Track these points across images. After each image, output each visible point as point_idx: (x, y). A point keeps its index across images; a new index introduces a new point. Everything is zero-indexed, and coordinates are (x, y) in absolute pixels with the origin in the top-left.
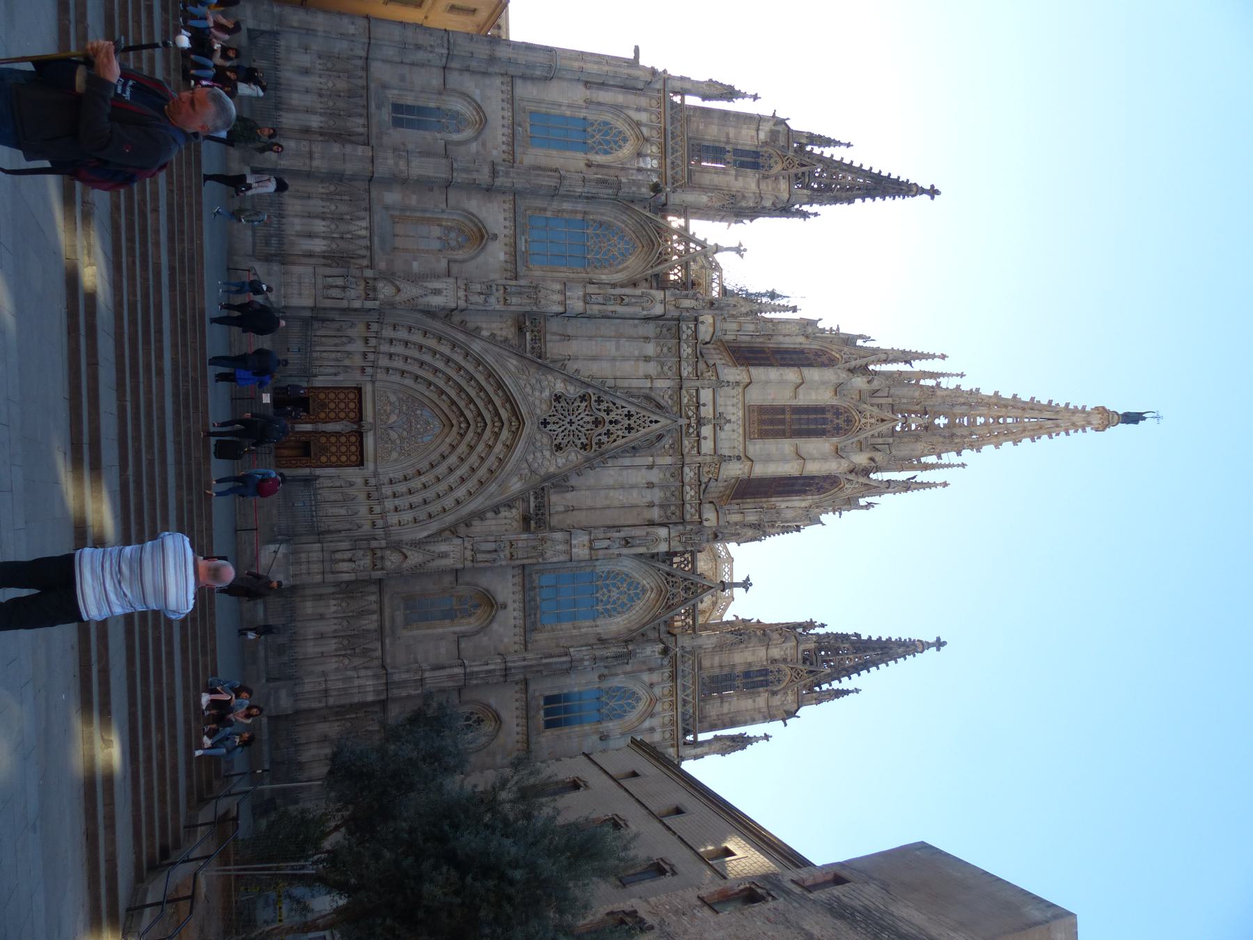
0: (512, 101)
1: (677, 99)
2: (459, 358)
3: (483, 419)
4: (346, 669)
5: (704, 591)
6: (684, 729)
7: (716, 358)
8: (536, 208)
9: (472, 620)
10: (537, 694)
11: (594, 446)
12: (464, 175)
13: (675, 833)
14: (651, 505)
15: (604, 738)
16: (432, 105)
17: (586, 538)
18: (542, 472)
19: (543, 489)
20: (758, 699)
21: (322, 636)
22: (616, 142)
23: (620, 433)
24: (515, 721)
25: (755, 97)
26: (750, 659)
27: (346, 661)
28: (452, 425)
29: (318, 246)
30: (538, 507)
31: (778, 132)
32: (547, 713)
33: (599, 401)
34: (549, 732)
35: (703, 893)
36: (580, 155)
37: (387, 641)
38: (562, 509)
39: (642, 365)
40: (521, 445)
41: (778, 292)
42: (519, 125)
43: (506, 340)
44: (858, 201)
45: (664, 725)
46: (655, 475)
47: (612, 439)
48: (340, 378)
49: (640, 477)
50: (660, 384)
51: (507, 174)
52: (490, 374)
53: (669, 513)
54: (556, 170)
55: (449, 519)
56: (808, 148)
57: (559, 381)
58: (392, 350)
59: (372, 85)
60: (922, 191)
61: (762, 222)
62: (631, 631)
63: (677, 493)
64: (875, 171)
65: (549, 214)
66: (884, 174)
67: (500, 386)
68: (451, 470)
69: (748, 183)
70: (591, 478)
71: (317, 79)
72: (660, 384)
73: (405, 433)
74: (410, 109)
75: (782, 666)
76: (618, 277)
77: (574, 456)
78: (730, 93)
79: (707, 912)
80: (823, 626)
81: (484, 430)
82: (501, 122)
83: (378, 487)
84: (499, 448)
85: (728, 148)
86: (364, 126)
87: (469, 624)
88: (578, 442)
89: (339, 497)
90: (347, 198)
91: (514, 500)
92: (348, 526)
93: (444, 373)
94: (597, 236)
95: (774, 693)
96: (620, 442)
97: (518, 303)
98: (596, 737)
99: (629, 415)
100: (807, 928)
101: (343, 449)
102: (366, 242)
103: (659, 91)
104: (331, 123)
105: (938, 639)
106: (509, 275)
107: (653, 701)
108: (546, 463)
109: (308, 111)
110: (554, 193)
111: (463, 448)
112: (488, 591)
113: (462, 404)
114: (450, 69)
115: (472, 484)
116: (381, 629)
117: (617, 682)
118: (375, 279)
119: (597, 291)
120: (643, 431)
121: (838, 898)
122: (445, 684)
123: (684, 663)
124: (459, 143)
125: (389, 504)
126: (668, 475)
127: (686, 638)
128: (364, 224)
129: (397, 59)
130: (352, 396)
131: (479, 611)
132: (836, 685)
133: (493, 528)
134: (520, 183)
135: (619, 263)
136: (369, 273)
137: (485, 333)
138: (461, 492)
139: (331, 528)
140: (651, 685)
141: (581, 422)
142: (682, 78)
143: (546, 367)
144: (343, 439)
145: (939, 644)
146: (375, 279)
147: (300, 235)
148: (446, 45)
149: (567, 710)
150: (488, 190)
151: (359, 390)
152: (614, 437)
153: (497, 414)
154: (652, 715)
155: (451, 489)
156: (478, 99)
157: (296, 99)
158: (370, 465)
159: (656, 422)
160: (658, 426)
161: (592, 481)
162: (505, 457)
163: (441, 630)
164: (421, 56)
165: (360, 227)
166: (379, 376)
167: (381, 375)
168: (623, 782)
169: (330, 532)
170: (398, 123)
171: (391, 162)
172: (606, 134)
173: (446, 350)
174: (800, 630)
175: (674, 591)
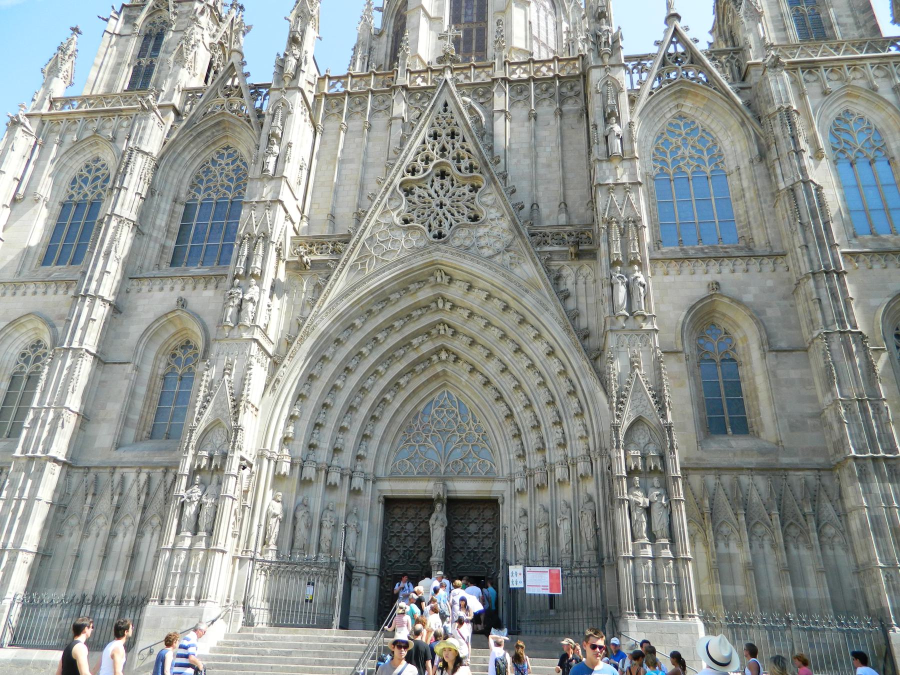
3: (433, 325)
9: (737, 335)
14: (561, 113)
17: (604, 165)
19: (533, 235)
22: (98, 170)
23: (457, 145)
27: (830, 530)
30: (562, 242)
33: (413, 171)
37: (785, 460)
39: (374, 133)
45: (889, 76)
46: (521, 112)
47: (466, 154)
48: (365, 525)
53: (572, 93)
55: (578, 362)
58: (325, 445)
62: (743, 124)
68: (505, 369)
73: (454, 439)
82: (39, 296)
83: (529, 474)
84: (475, 300)
87: (745, 339)
88: (469, 195)
89: (542, 534)
91: (548, 271)
92: (587, 519)
93: (365, 378)
99: (435, 136)
101: (473, 528)
107: (850, 92)
108: (495, 232)
111: (476, 355)
113: (413, 356)
119: (259, 165)
120: (457, 119)
125: (555, 455)
126: (520, 97)
128: (131, 476)
130: (398, 512)
131: (723, 325)
133: (591, 300)
135: (245, 164)
138: (537, 350)
139: (591, 546)
141: (441, 193)
144: (459, 528)
147: (129, 575)
151: (390, 503)
152: (463, 153)
155: (532, 366)
158: (496, 488)
159: (446, 105)
165: (134, 481)
166: (369, 469)
167: (368, 466)
169: (598, 548)
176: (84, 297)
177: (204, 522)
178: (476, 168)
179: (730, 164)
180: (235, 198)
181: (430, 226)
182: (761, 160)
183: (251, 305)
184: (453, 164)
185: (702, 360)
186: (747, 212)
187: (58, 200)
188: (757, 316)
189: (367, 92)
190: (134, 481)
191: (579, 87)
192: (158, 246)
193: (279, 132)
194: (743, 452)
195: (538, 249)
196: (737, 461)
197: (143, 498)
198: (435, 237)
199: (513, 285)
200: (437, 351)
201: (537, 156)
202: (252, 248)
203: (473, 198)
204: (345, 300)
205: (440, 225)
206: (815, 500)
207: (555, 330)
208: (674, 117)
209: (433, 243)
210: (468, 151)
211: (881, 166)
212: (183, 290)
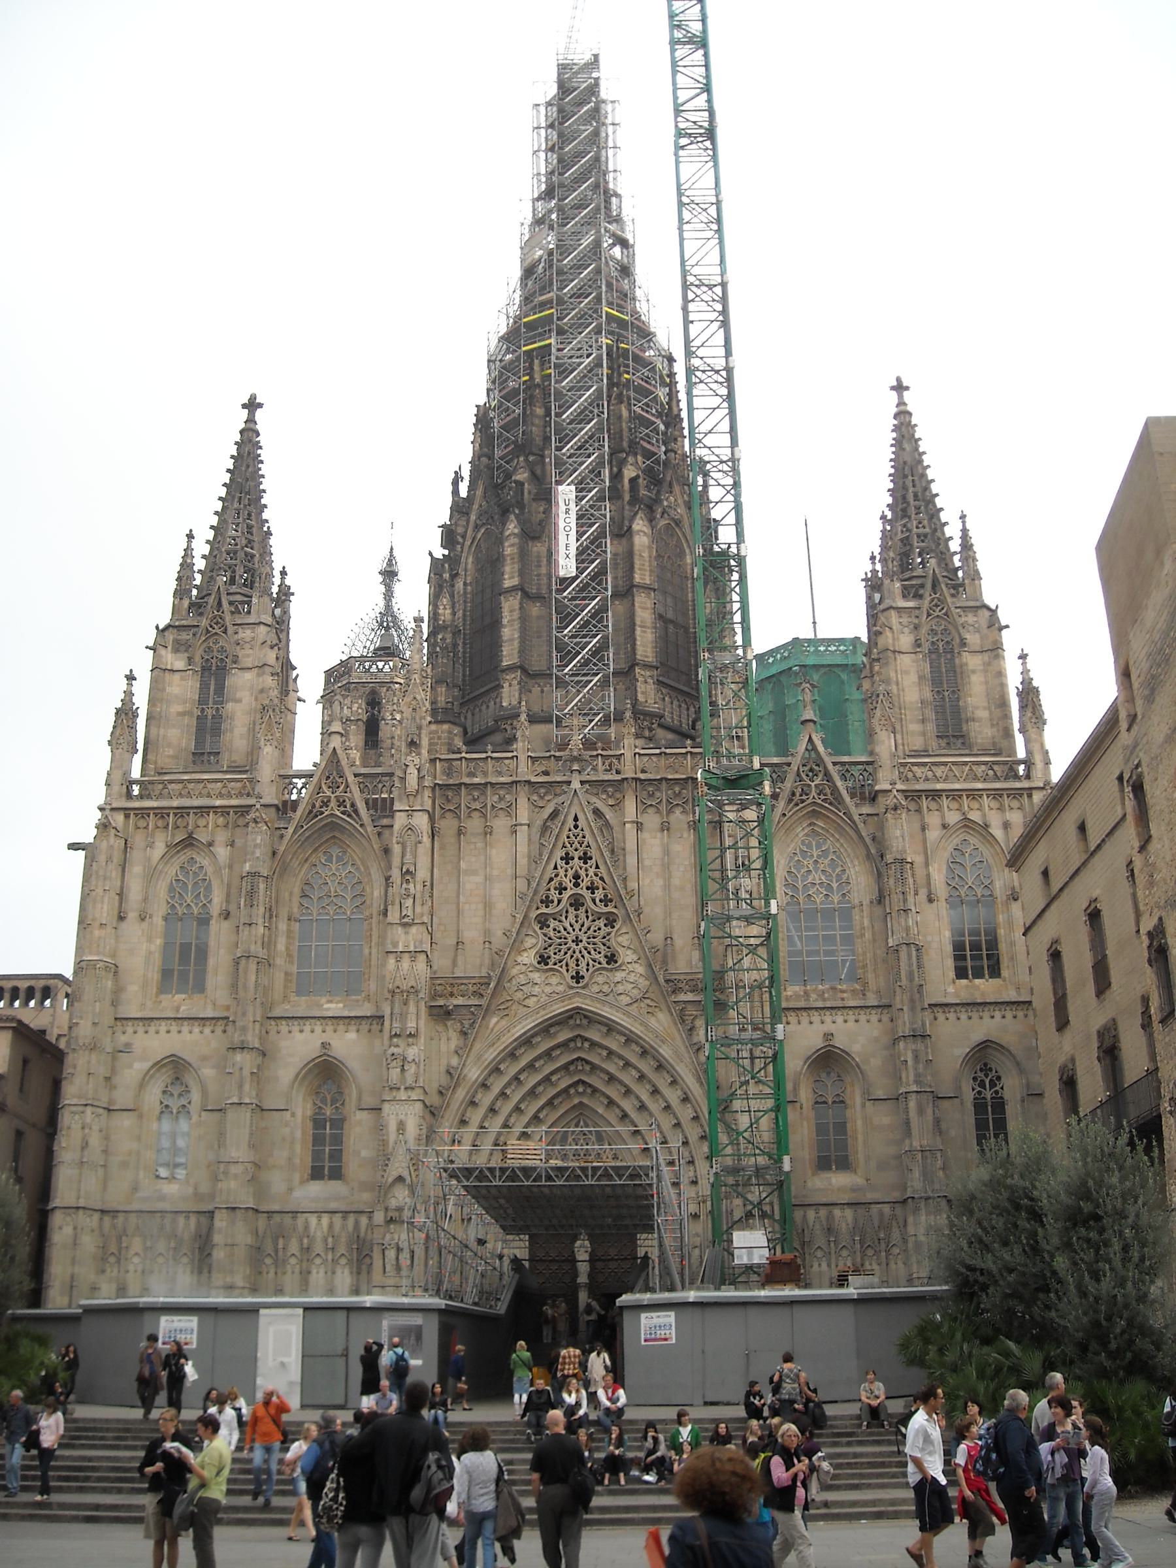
1: (136, 790)
2: (485, 1100)
3: (572, 1062)
5: (814, 748)
6: (1006, 778)
7: (486, 714)
8: (285, 987)
9: (848, 1079)
10: (951, 989)
11: (610, 909)
12: (247, 1087)
13: (1103, 840)
18: (643, 983)
19: (667, 981)
20: (971, 667)
23: (591, 873)
24: (987, 1019)
25: (131, 678)
26: (913, 677)
28: (581, 1102)
31: (177, 642)
32: (978, 974)
33: (547, 902)
34: (1005, 973)
35: (1137, 845)
37: (870, 1196)
38: (696, 955)
40: (607, 1012)
41: (381, 565)
42: (178, 1009)
43: (465, 1034)
44: (265, 516)
45: (1001, 809)
49: (654, 843)
50: (523, 814)
51: (244, 1029)
52: (512, 1056)
54: (237, 962)
56: (195, 592)
57: (519, 959)
59: (136, 1206)
60: (251, 420)
61: (291, 657)
62: (869, 855)
63: (677, 789)
64: (223, 492)
66: (226, 478)
67: (526, 1041)
69: (244, 686)
70: (654, 913)
71: (131, 1275)
72: (523, 814)
75: (924, 630)
77: (622, 940)
78: (125, 714)
81: (587, 1062)
86: (187, 1218)
90: (281, 1241)
95: (963, 643)
96: (603, 870)
97: (416, 1018)
99: (567, 858)
102: (337, 1219)
103: (127, 816)
105: (893, 388)
106: (376, 1027)
108: (632, 978)
110: (266, 963)
111: (613, 1092)
112: (809, 1058)
114: (111, 1101)
115: (662, 1082)
117: (938, 876)
118: (387, 1209)
120: (589, 838)
121: (1141, 685)
122: (930, 1118)
123: (917, 779)
124: (204, 1093)
127: (881, 774)
128: (313, 1220)
129: (101, 1171)
132: (955, 546)
134: (254, 1013)
136: (379, 1217)
137: (455, 1061)
138: (673, 1096)
140: (944, 826)
141: (577, 927)
142: (108, 784)
143: (499, 979)
145: (900, 388)
146: (387, 1209)
148: (81, 1109)
149: (976, 946)
150: (264, 1055)
153: (564, 1045)
154: (986, 826)
155: (668, 1108)
156: (146, 1065)
159: (576, 819)
160: (581, 816)
161: (658, 910)
162: (625, 1035)
163: (859, 1123)
164: (95, 1141)
165: (318, 1226)
168: (1055, 888)
171: (233, 1184)
173: (476, 1117)
174: (877, 597)
175: (813, 793)
178: (611, 901)
179: (855, 898)
180: (352, 913)
181: (567, 965)
182: (879, 902)
183: (413, 1066)
184: (587, 894)
185: (817, 1103)
186: (864, 953)
187: (161, 914)
189: (486, 784)
192: (282, 975)
193: (412, 869)
194: (841, 1189)
195: (673, 998)
197: (330, 1240)
198: (572, 977)
199: (650, 1035)
200: (574, 1085)
201: (670, 877)
203: (609, 934)
204: (491, 1050)
205: (577, 965)
206: (888, 1228)
208: (806, 835)
209: (572, 988)
210: (602, 879)
212: (324, 1032)
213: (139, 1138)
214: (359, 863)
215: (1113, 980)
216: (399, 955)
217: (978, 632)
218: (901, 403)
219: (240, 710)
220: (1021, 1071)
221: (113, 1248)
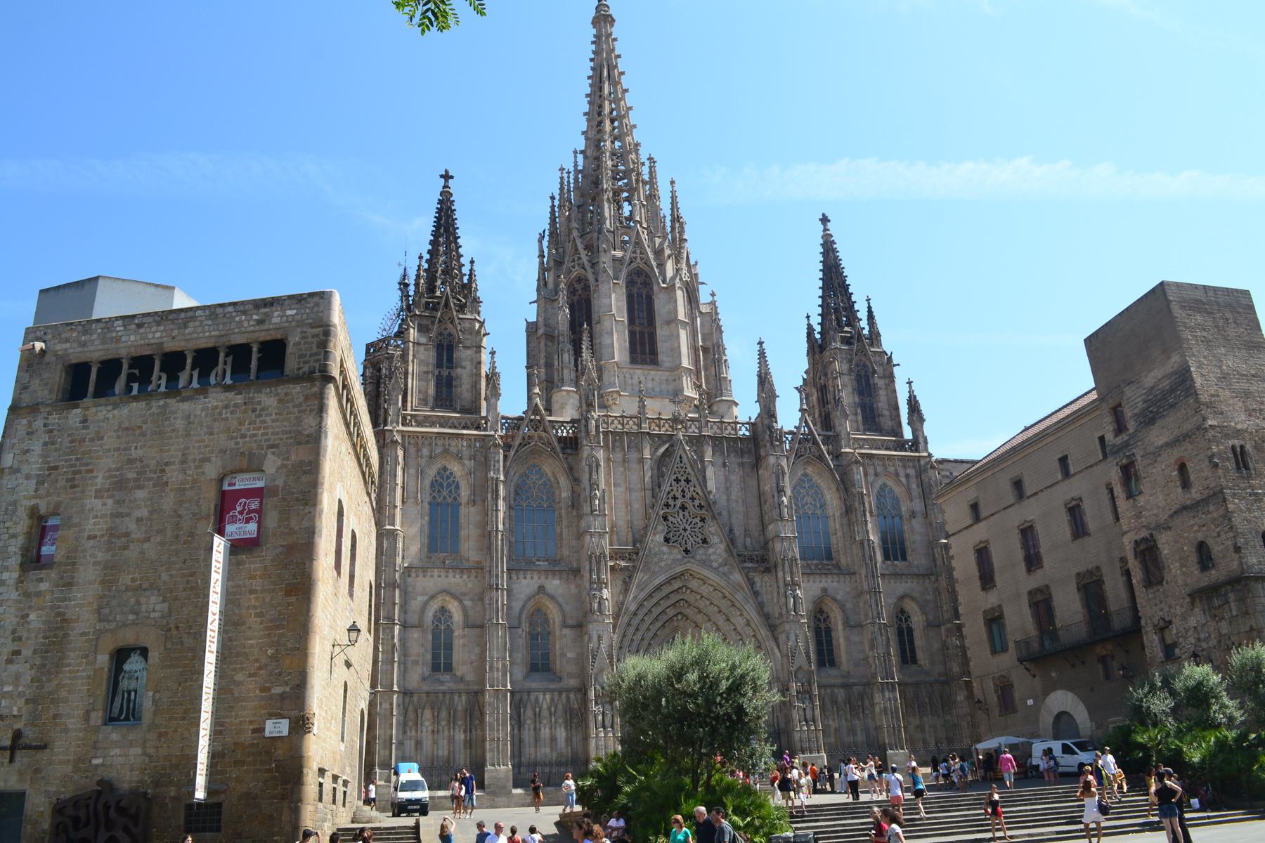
0: (424, 570)
4: (873, 712)
9: (832, 615)
14: (742, 465)
15: (913, 514)
16: (430, 637)
18: (725, 555)
21: (852, 731)
22: (448, 478)
29: (561, 733)
30: (751, 559)
33: (667, 505)
34: (909, 558)
36: (463, 511)
40: (706, 572)
45: (905, 467)
52: (650, 596)
59: (425, 688)
60: (446, 186)
65: (513, 539)
67: (658, 588)
74: (435, 656)
76: (564, 482)
77: (712, 528)
79: (1141, 500)
80: (808, 317)
84: (705, 590)
85: (436, 372)
88: (700, 524)
94: (528, 498)
95: (874, 372)
98: (913, 521)
99: (677, 480)
100: (1160, 443)
104: (459, 723)
107: (887, 474)
109: (451, 740)
113: (665, 618)
116: (845, 686)
120: (689, 470)
121: (1136, 415)
128: (541, 697)
131: (825, 609)
137: (621, 598)
140: (876, 475)
145: (825, 220)
149: (894, 543)
154: (897, 475)
156: (425, 598)
157: (443, 752)
160: (684, 456)
165: (545, 700)
170: (449, 668)
172: (441, 485)
176: (497, 589)
177: (608, 723)
179: (830, 512)
188: (842, 607)
190: (545, 700)
191: (752, 446)
196: (832, 681)
202: (598, 563)
206: (862, 699)
207: (751, 611)
211: (897, 520)
213: (423, 645)
214: (550, 475)
215: (1046, 565)
216: (592, 535)
217: (881, 365)
218: (825, 230)
219: (463, 373)
220: (924, 613)
221: (411, 715)
